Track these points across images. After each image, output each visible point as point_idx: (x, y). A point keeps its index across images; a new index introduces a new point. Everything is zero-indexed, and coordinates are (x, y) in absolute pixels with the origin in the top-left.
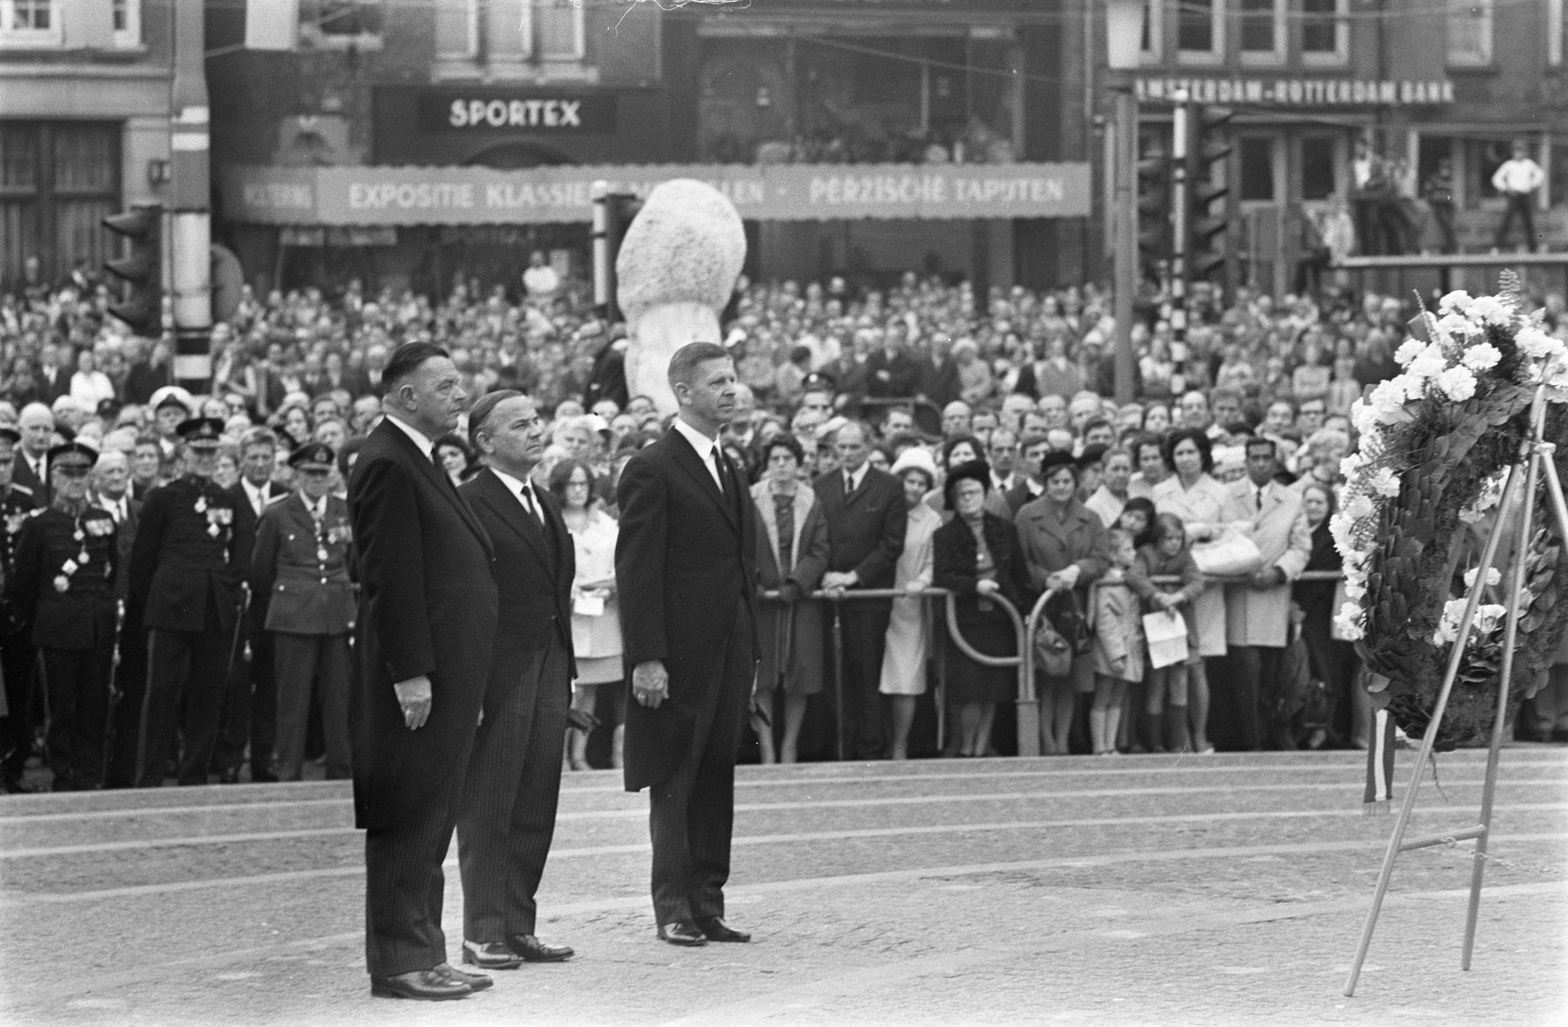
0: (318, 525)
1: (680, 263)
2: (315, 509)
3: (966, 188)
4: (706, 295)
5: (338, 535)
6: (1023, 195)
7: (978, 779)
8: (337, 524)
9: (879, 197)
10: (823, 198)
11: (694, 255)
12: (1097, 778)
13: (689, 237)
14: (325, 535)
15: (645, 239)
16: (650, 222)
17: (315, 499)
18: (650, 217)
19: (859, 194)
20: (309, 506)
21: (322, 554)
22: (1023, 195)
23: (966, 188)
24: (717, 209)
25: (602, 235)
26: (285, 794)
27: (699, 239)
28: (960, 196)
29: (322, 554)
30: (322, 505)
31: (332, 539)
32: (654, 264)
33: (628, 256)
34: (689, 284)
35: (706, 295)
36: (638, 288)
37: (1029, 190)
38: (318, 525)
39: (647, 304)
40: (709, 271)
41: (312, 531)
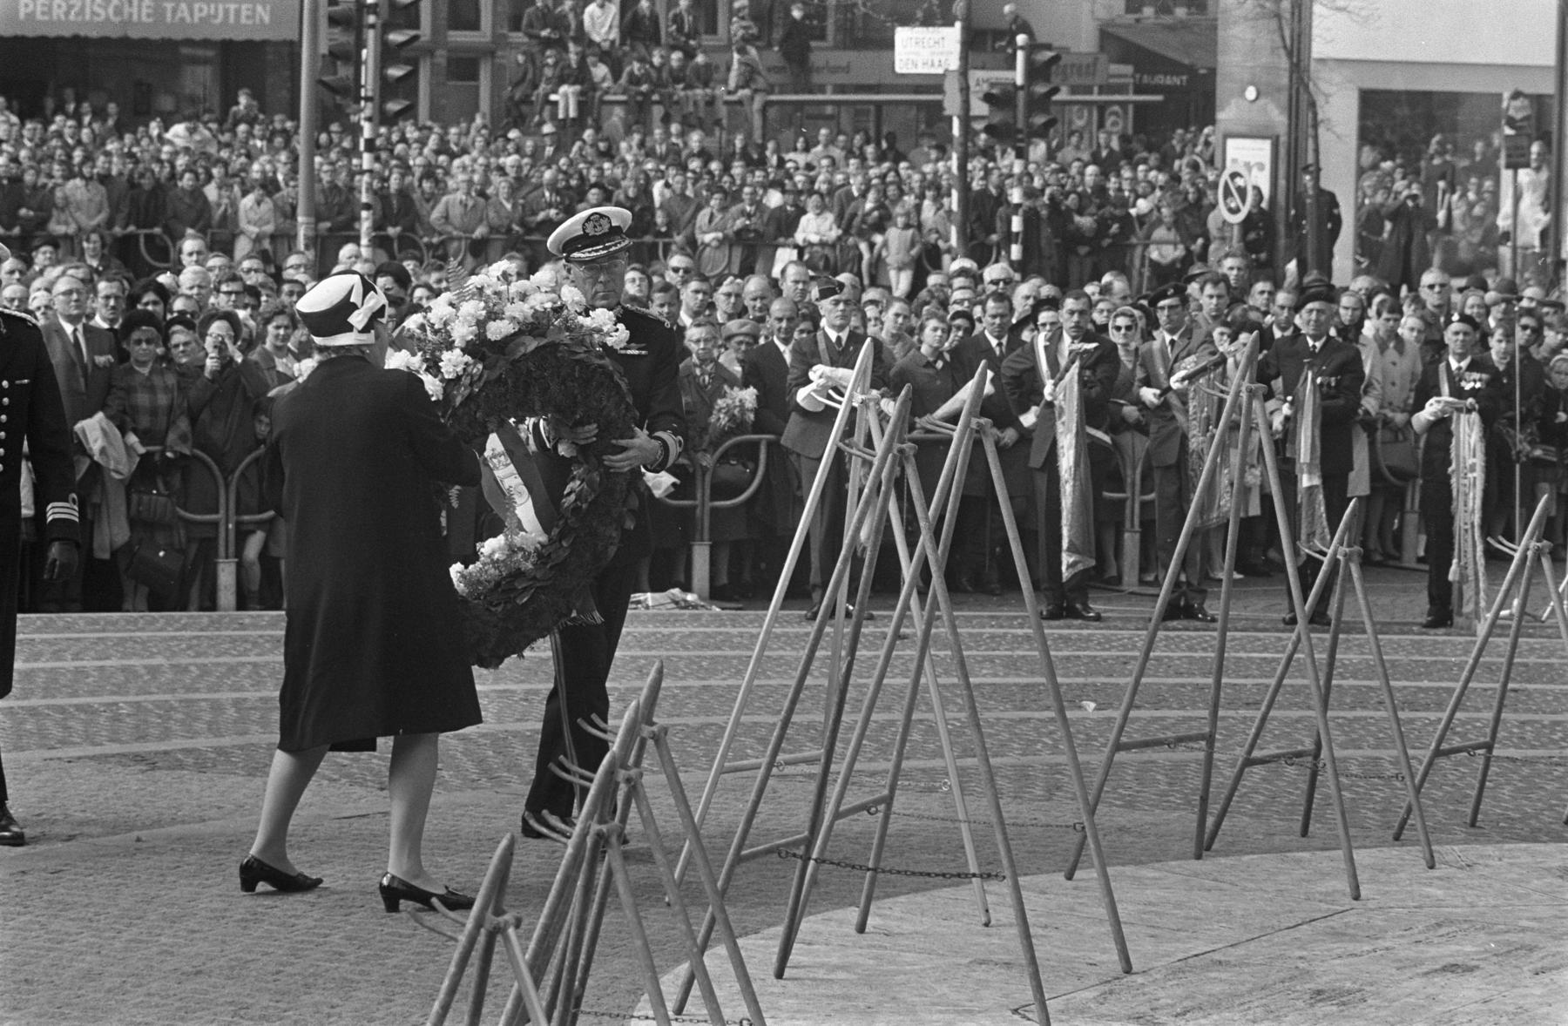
3: (174, 11)
6: (232, 19)
10: (31, 16)
19: (67, 14)
22: (232, 19)
23: (174, 11)
37: (238, 12)
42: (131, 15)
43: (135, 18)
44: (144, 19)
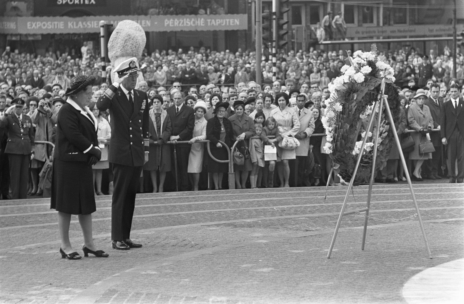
0: (20, 122)
1: (126, 45)
2: (19, 117)
3: (211, 22)
4: (134, 54)
5: (26, 125)
6: (228, 24)
7: (217, 196)
8: (26, 122)
9: (185, 25)
10: (168, 25)
11: (131, 42)
12: (252, 195)
13: (129, 37)
14: (23, 125)
15: (116, 38)
16: (117, 33)
17: (19, 115)
18: (118, 31)
19: (179, 24)
20: (18, 117)
21: (22, 131)
22: (228, 24)
23: (211, 22)
24: (138, 29)
25: (103, 37)
26: (12, 203)
27: (132, 38)
28: (209, 24)
29: (22, 131)
30: (21, 116)
31: (25, 126)
32: (119, 45)
33: (111, 43)
34: (129, 51)
35: (134, 54)
36: (114, 52)
37: (229, 22)
38: (20, 122)
39: (117, 57)
40: (135, 47)
41: (19, 124)
42: (198, 24)
43: (199, 24)
44: (202, 25)
